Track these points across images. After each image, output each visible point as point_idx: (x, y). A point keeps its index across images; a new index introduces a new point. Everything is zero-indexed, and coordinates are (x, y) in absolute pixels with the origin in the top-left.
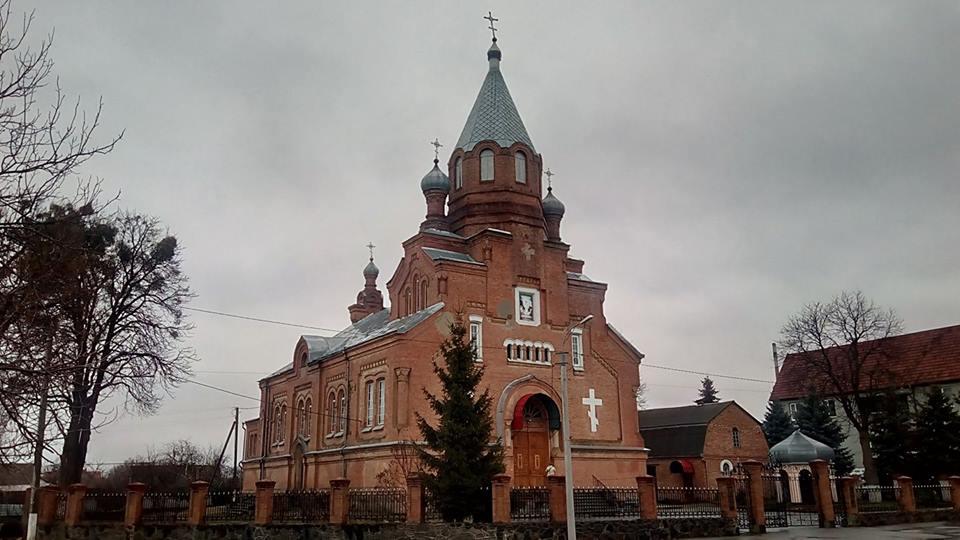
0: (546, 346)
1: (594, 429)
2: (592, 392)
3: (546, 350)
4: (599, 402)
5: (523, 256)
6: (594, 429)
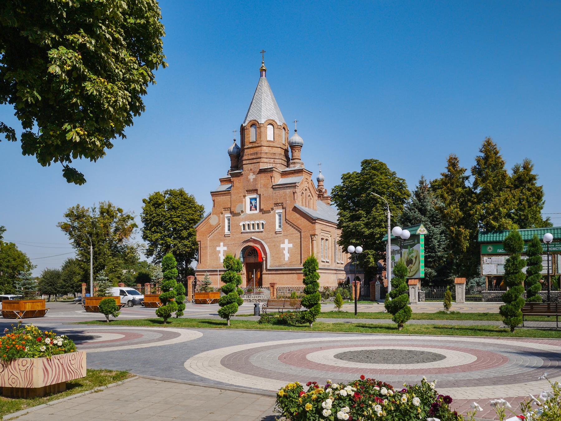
0: (261, 222)
1: (286, 259)
2: (286, 241)
3: (263, 224)
4: (291, 245)
5: (249, 181)
6: (286, 259)
